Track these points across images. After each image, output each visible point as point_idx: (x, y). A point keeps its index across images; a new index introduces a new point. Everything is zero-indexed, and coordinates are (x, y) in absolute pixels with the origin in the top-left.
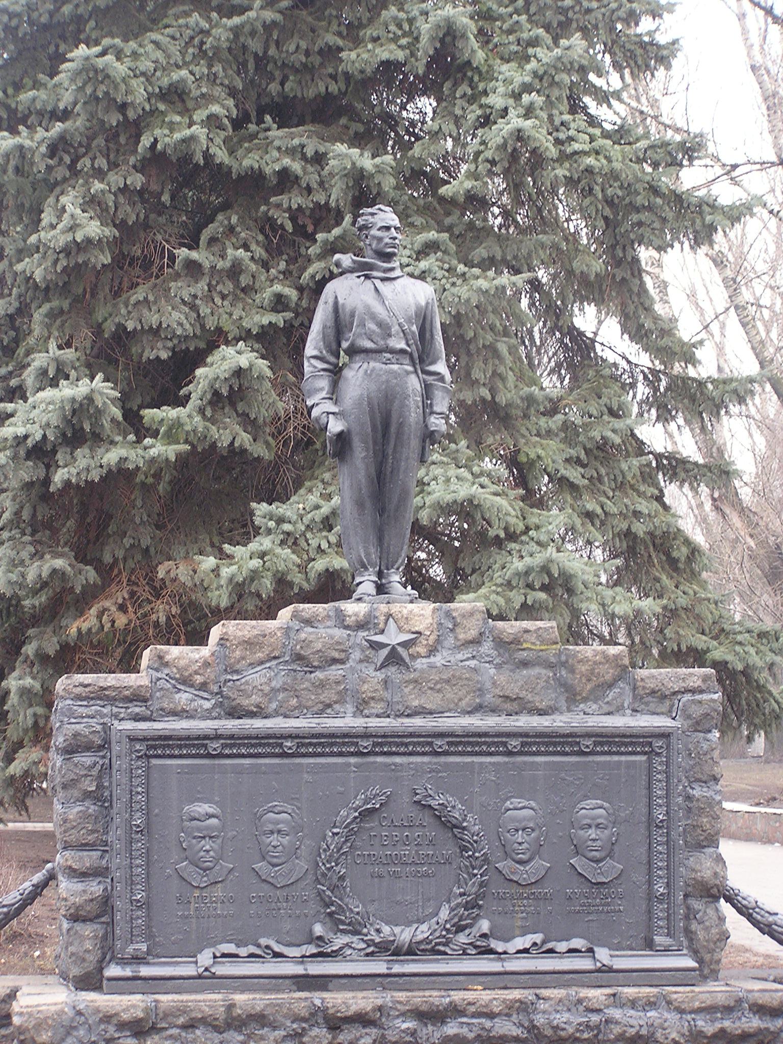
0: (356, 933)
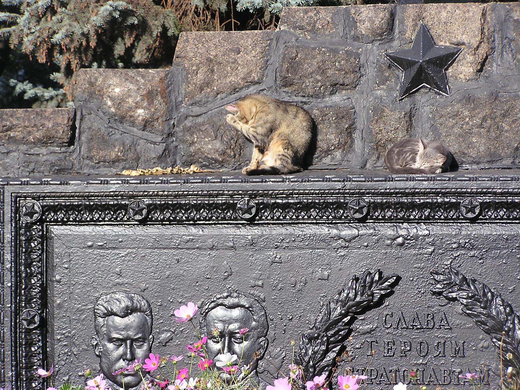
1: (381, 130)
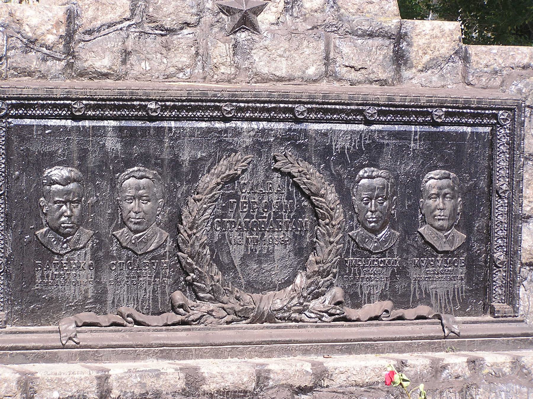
1: (217, 56)
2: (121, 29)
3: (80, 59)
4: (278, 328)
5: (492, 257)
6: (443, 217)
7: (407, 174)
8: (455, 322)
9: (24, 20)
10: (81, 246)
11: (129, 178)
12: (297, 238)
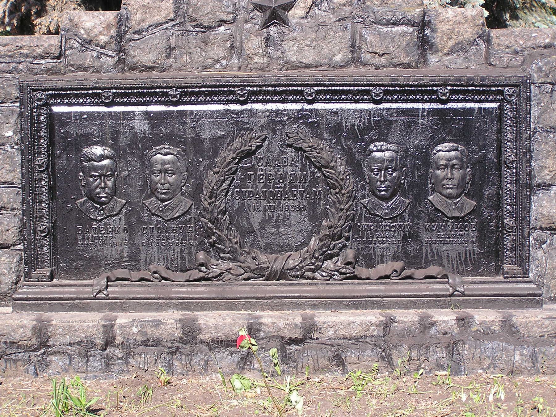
0: (234, 260)
2: (167, 29)
3: (130, 56)
4: (290, 284)
5: (503, 222)
6: (451, 186)
7: (416, 147)
8: (463, 283)
9: (80, 24)
10: (115, 213)
11: (156, 155)
12: (313, 206)
